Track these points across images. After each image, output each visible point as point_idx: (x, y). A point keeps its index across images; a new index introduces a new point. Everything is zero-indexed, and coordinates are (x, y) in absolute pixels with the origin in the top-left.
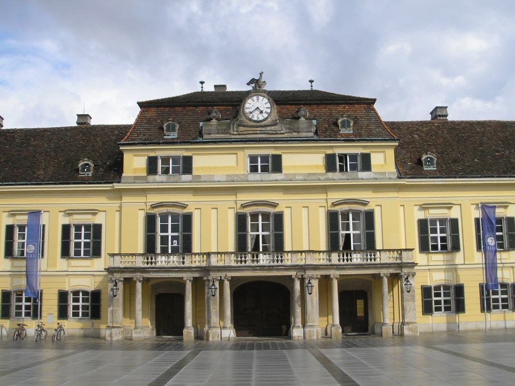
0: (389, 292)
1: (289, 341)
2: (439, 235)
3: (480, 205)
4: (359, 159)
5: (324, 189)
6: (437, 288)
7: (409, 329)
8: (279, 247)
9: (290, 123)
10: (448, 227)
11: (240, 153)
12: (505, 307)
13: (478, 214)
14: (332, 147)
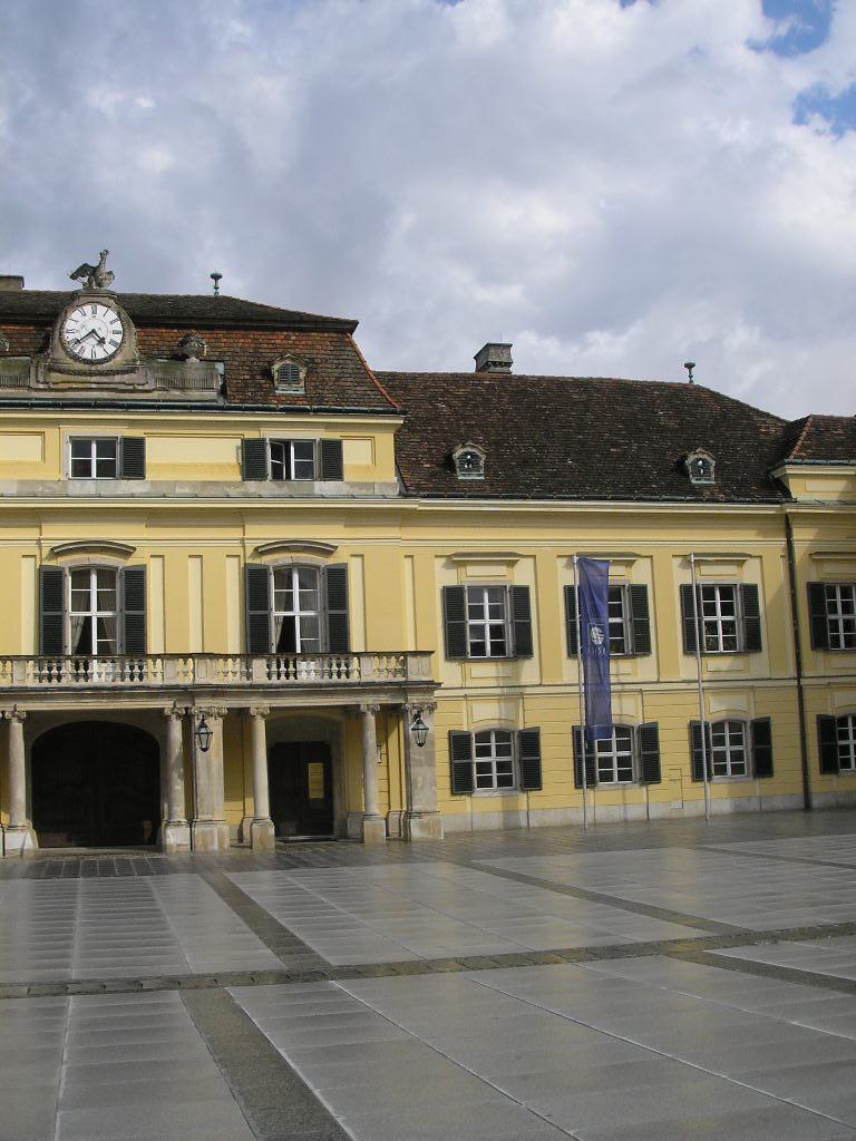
0: (379, 746)
1: (157, 856)
2: (487, 622)
3: (576, 559)
4: (316, 452)
5: (239, 517)
6: (483, 736)
7: (423, 827)
8: (135, 645)
9: (165, 369)
10: (508, 604)
11: (51, 432)
12: (625, 776)
13: (570, 577)
14: (257, 425)
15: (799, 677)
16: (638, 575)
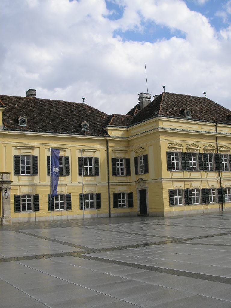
2: (26, 165)
3: (50, 149)
6: (24, 196)
7: (6, 221)
10: (31, 160)
12: (62, 208)
13: (49, 154)
15: (109, 182)
16: (67, 154)
